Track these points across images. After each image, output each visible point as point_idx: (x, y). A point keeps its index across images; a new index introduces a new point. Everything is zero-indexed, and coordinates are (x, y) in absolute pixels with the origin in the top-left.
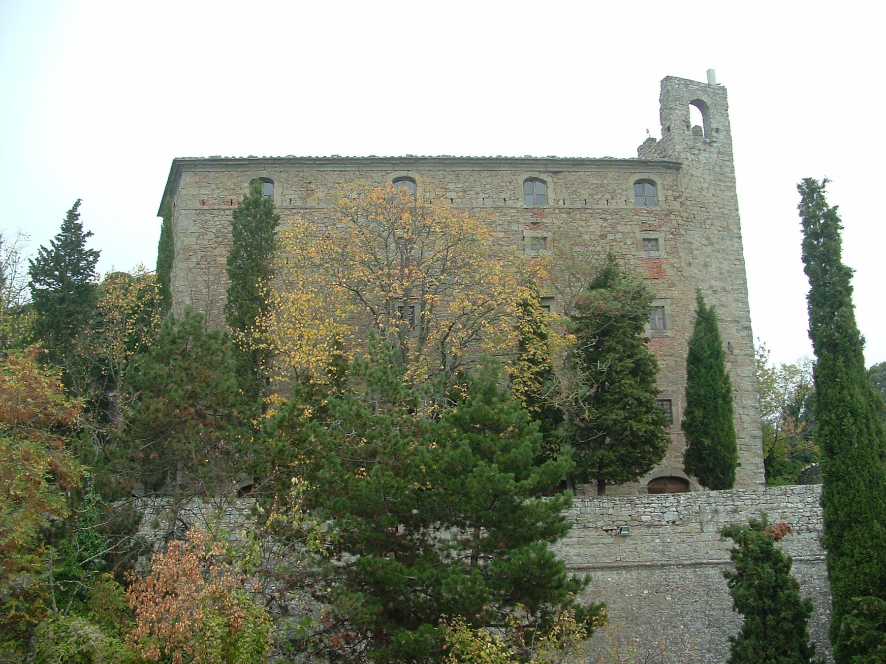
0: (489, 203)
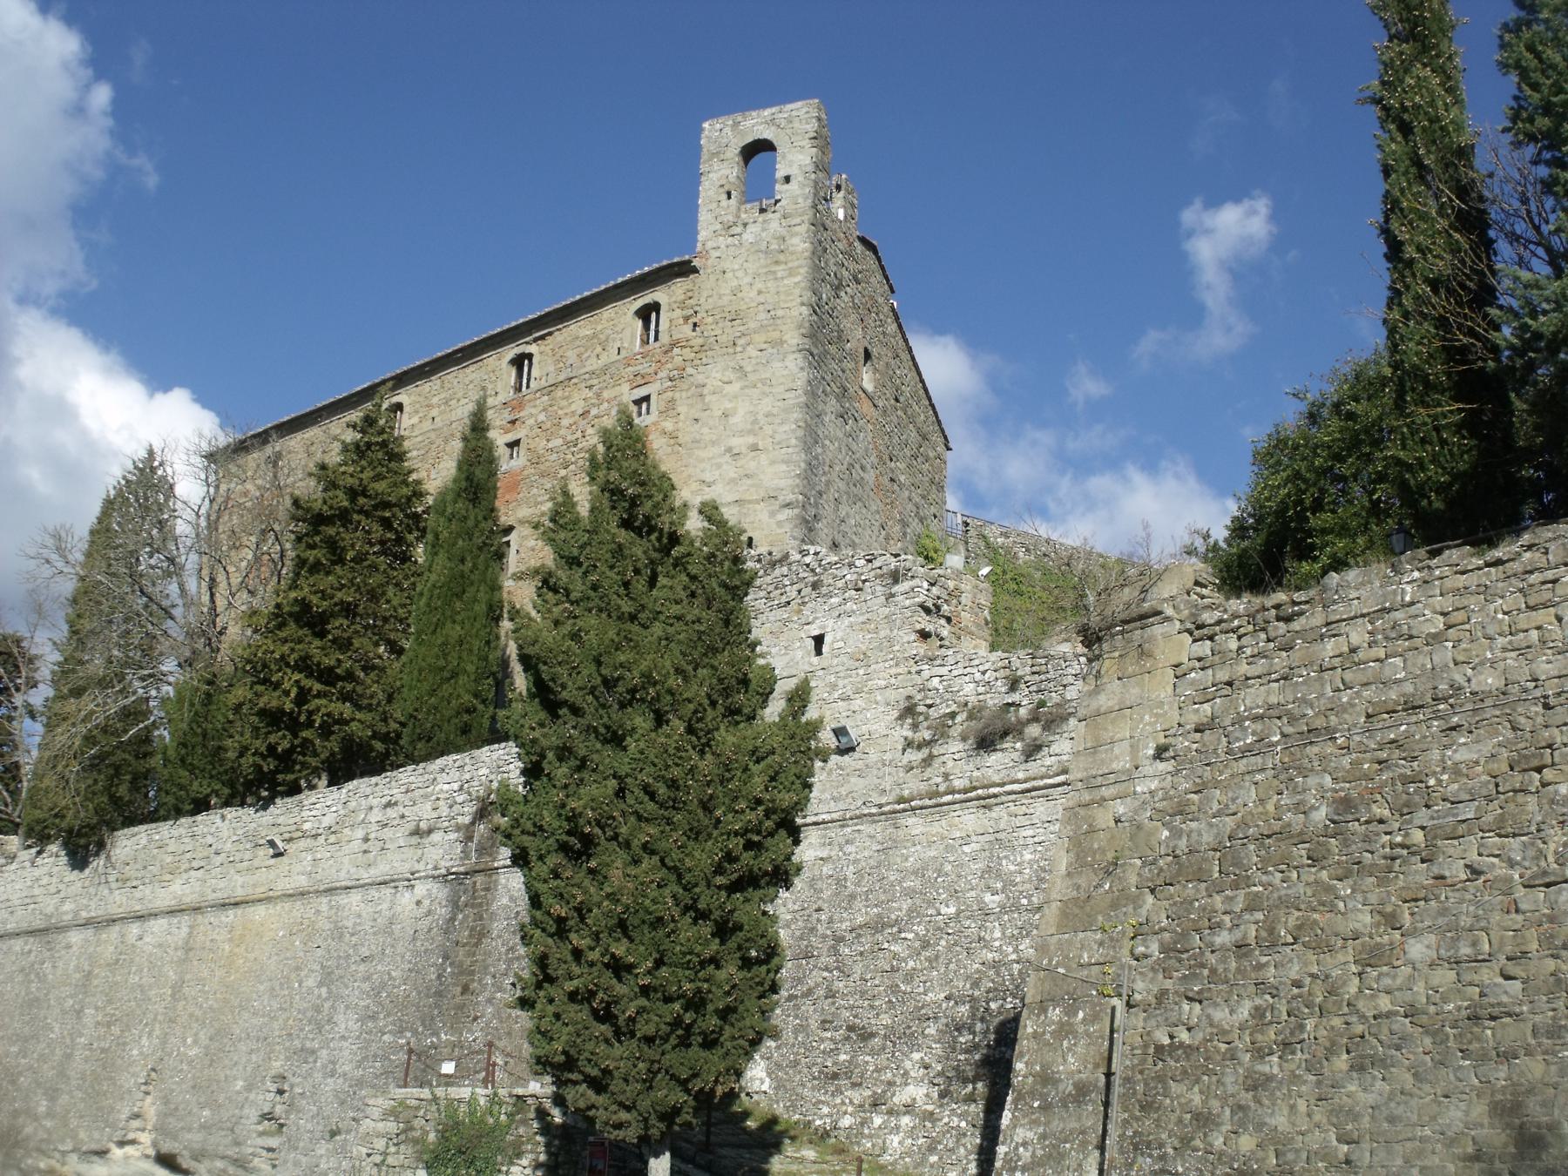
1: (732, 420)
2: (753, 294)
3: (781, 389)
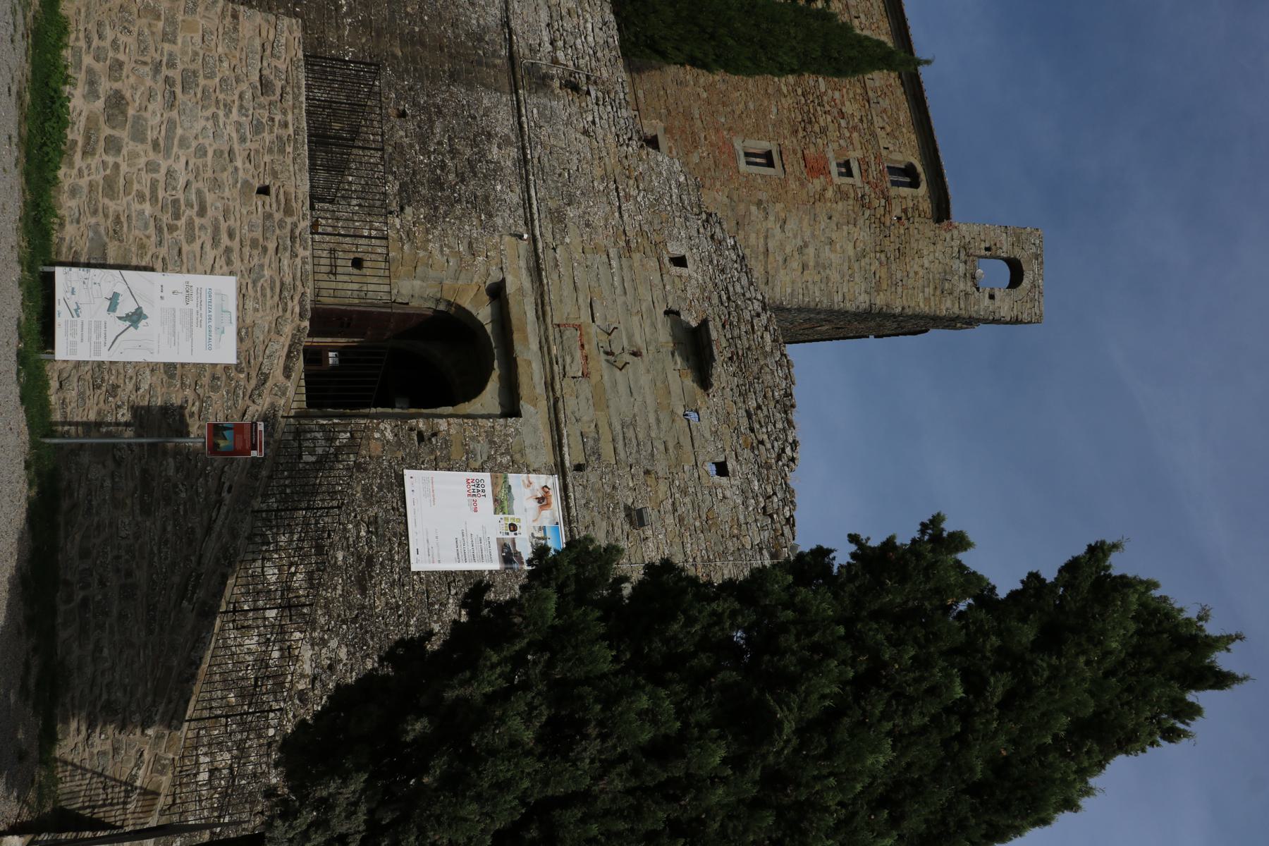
1: (827, 247)
2: (916, 268)
3: (845, 290)
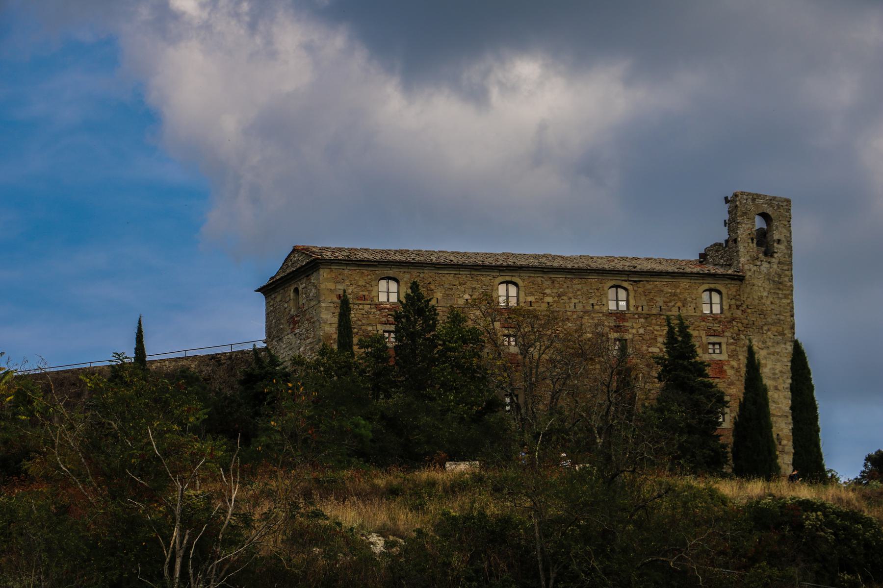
0: (579, 307)
2: (768, 303)
